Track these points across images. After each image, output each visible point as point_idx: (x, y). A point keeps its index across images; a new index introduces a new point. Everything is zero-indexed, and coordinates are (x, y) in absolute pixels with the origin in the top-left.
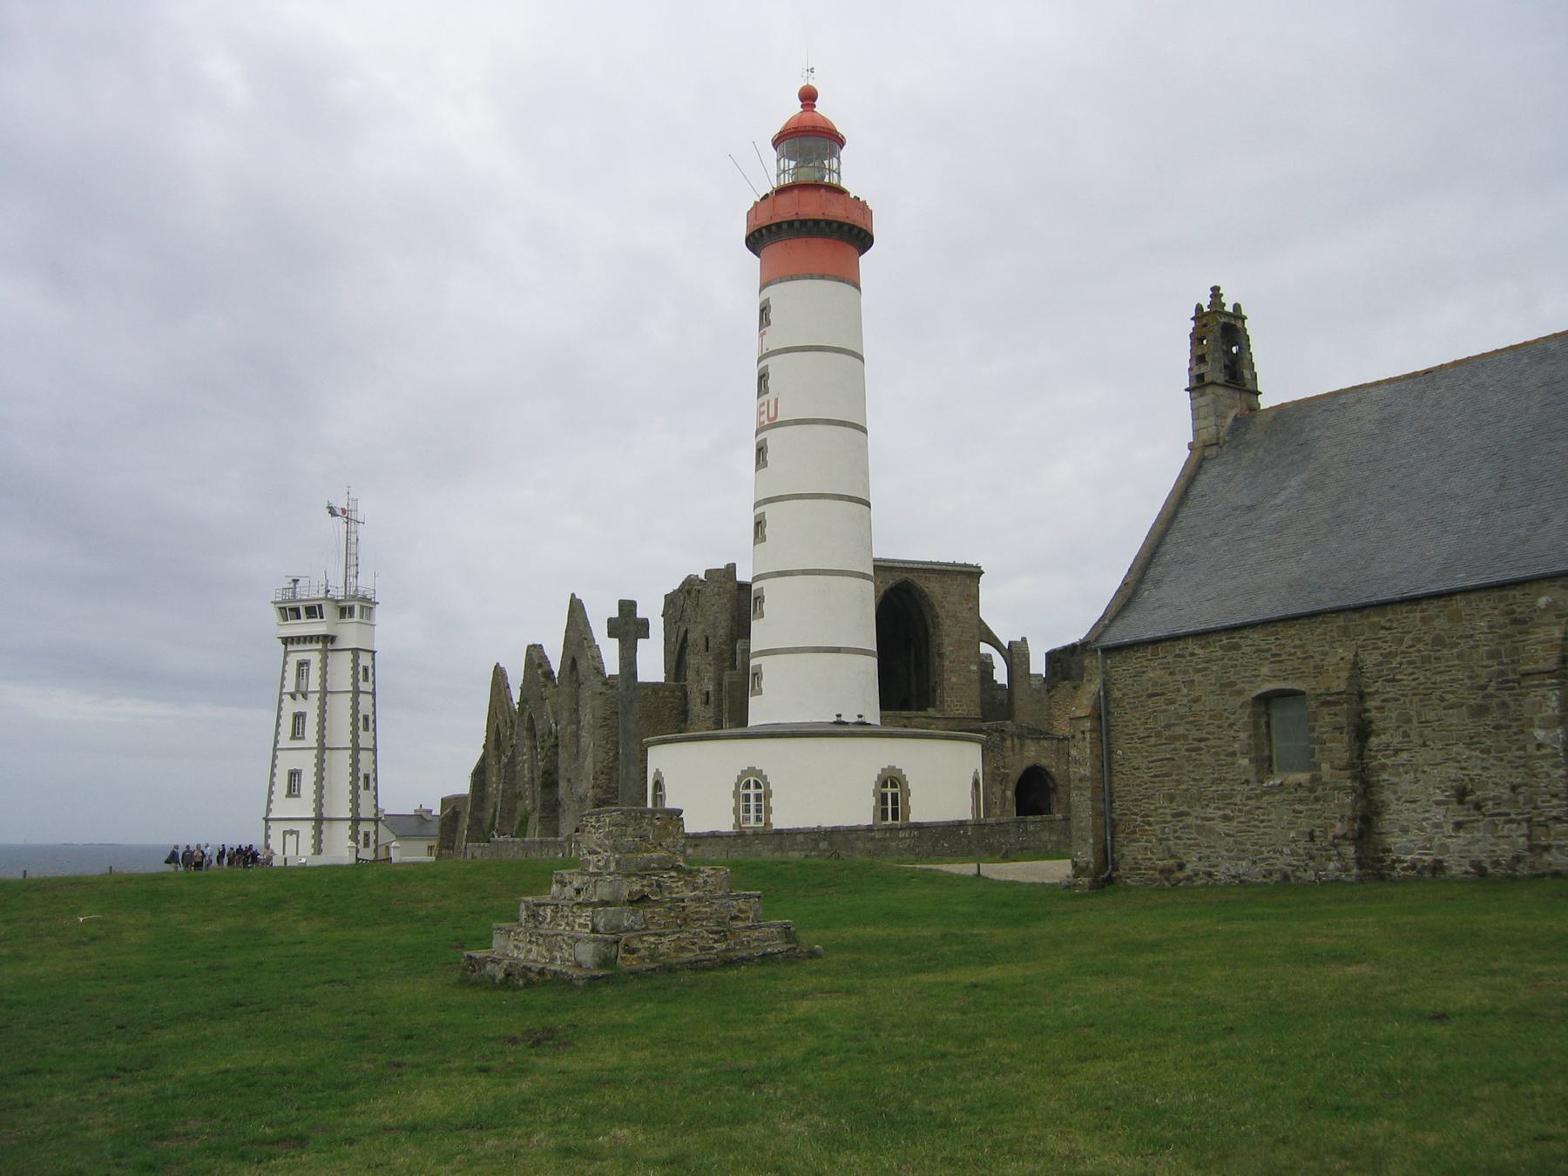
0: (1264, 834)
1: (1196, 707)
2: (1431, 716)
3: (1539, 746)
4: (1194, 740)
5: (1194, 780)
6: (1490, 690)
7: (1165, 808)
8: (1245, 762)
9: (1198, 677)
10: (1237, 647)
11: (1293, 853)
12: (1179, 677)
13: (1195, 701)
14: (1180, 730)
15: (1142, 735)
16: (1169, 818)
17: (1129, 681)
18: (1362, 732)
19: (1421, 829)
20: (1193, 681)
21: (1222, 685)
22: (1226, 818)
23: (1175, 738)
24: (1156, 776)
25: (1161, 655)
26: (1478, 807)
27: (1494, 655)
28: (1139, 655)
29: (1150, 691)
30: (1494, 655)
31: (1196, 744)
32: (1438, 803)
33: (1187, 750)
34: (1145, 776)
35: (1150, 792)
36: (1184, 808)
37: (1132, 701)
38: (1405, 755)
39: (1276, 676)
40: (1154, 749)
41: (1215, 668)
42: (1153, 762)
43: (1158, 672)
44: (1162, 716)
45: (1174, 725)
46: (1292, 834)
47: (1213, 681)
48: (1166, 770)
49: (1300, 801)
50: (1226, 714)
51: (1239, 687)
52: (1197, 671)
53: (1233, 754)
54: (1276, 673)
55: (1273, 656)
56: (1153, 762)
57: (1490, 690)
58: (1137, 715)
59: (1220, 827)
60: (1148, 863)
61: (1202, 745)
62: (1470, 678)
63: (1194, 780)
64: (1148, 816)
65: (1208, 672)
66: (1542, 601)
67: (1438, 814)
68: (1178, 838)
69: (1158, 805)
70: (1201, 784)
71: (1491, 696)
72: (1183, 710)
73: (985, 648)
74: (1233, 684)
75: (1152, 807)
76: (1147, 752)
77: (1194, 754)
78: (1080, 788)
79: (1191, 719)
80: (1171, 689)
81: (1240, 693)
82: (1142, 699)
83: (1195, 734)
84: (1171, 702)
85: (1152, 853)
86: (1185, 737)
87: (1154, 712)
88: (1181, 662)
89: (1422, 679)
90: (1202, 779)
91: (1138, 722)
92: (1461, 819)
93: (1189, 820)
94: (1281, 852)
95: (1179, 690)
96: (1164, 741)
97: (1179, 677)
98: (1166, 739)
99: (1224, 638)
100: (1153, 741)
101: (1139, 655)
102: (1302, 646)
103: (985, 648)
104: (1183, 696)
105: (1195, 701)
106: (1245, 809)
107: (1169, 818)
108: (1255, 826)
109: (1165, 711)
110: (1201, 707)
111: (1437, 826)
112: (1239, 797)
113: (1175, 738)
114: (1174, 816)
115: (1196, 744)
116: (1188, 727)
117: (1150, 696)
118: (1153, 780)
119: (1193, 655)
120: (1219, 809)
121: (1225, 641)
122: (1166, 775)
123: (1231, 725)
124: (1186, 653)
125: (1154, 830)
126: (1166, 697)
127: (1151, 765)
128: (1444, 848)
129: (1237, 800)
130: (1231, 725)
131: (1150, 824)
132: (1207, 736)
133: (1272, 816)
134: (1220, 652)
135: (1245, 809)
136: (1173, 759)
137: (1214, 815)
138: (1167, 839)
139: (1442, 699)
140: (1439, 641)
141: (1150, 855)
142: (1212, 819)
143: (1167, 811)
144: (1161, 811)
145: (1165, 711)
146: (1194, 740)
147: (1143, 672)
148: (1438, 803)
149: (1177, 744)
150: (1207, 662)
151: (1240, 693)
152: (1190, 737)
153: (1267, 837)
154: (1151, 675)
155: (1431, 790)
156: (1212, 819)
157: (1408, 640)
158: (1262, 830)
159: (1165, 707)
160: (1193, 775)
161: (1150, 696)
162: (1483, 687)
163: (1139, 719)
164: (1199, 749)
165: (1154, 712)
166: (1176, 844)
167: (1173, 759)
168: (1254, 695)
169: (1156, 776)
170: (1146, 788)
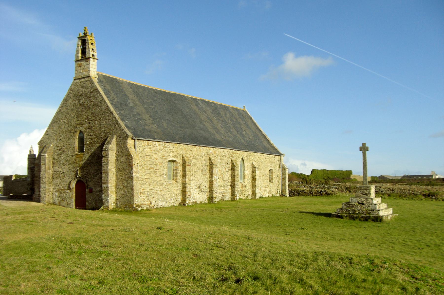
0: (168, 195)
1: (157, 161)
2: (196, 170)
4: (156, 169)
5: (155, 180)
6: (204, 167)
7: (148, 187)
8: (165, 176)
9: (157, 153)
10: (166, 147)
11: (174, 199)
12: (153, 152)
13: (157, 159)
14: (152, 166)
15: (144, 166)
16: (149, 190)
17: (141, 150)
20: (156, 154)
21: (162, 156)
22: (161, 190)
23: (151, 168)
24: (146, 178)
25: (149, 145)
26: (201, 190)
29: (146, 154)
31: (156, 171)
32: (196, 189)
33: (154, 172)
35: (145, 183)
36: (152, 188)
37: (141, 156)
41: (161, 151)
42: (146, 174)
43: (149, 150)
44: (148, 162)
46: (173, 195)
48: (149, 177)
50: (162, 164)
51: (166, 157)
52: (157, 151)
53: (163, 174)
55: (173, 151)
56: (146, 174)
57: (204, 167)
58: (143, 160)
59: (160, 193)
60: (144, 203)
61: (157, 171)
62: (202, 164)
64: (144, 189)
65: (160, 152)
66: (211, 151)
68: (151, 196)
70: (156, 181)
74: (164, 156)
75: (145, 187)
76: (144, 171)
77: (155, 173)
78: (137, 180)
79: (155, 164)
80: (151, 155)
81: (166, 159)
82: (144, 156)
83: (155, 168)
84: (151, 158)
85: (145, 200)
86: (154, 168)
87: (147, 160)
88: (154, 148)
89: (195, 163)
90: (156, 180)
91: (143, 162)
92: (199, 192)
93: (153, 191)
94: (171, 200)
95: (153, 155)
97: (153, 152)
98: (149, 168)
99: (164, 144)
100: (146, 168)
101: (144, 143)
102: (178, 150)
104: (153, 157)
105: (157, 159)
106: (165, 188)
107: (149, 190)
109: (150, 160)
110: (157, 161)
111: (196, 194)
112: (164, 185)
113: (151, 168)
115: (156, 171)
116: (154, 166)
117: (146, 155)
119: (157, 147)
120: (160, 188)
121: (164, 145)
123: (163, 167)
124: (155, 146)
125: (145, 193)
126: (150, 156)
129: (164, 186)
130: (163, 167)
131: (144, 192)
132: (158, 169)
134: (163, 148)
135: (165, 188)
136: (150, 174)
137: (158, 190)
138: (148, 196)
139: (198, 167)
141: (144, 201)
142: (158, 191)
143: (148, 188)
144: (147, 188)
145: (150, 160)
146: (156, 169)
147: (145, 148)
148: (196, 189)
149: (152, 170)
150: (159, 149)
151: (166, 159)
152: (155, 169)
154: (147, 150)
156: (158, 191)
158: (168, 194)
159: (149, 159)
160: (154, 179)
161: (146, 155)
162: (203, 166)
163: (143, 161)
164: (156, 172)
165: (147, 160)
166: (150, 197)
167: (150, 174)
168: (168, 160)
169: (146, 178)
170: (144, 182)
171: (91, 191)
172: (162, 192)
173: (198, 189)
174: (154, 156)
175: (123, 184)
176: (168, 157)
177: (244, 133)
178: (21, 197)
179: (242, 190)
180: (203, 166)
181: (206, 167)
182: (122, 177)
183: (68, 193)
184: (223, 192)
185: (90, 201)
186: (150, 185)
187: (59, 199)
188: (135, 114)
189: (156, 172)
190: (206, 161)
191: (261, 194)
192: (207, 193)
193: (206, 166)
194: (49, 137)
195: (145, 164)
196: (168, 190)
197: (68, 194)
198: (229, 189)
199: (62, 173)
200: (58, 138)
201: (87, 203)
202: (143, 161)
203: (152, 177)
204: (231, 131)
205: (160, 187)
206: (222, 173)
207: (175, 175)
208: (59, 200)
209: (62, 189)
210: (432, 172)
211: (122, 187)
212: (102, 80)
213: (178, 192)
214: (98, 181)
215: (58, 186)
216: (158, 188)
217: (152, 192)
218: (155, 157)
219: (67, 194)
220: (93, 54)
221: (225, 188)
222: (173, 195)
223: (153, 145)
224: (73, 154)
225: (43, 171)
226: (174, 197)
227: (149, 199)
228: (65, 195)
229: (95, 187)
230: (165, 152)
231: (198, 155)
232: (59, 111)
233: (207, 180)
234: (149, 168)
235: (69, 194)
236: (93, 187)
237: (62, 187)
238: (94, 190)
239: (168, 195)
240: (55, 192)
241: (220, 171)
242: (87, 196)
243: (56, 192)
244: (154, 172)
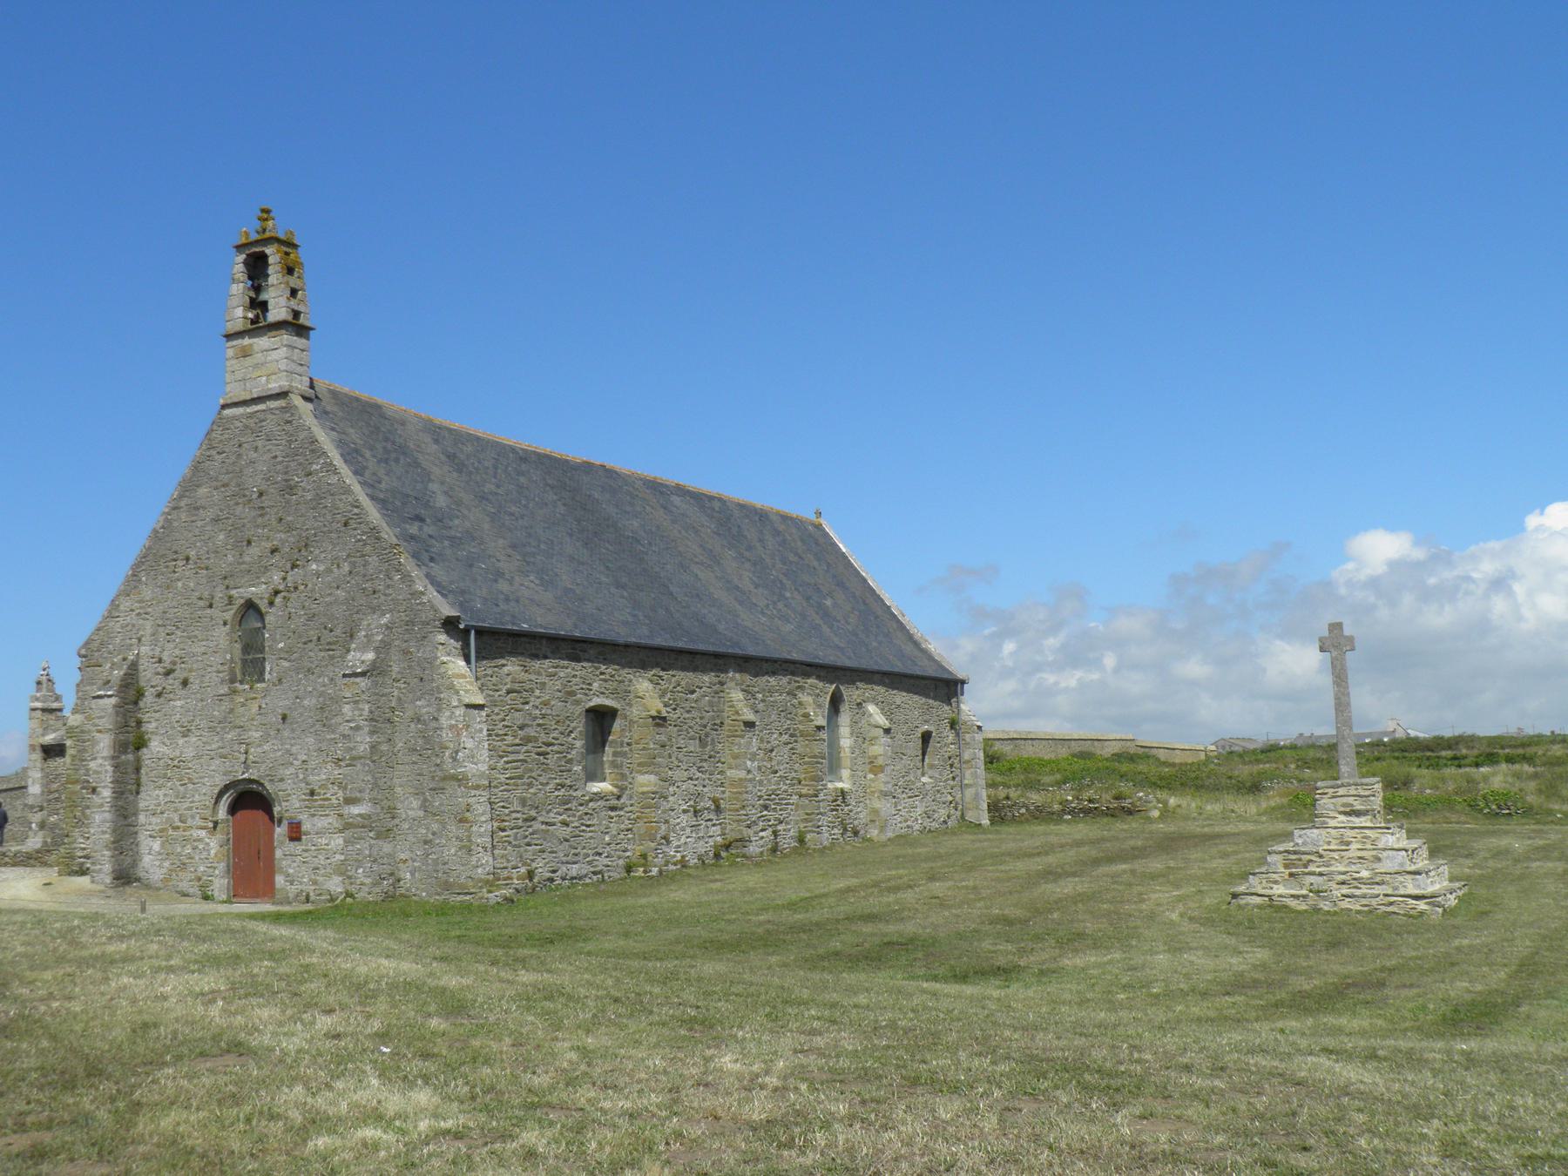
0: (591, 838)
2: (682, 743)
4: (543, 743)
5: (542, 784)
7: (518, 812)
13: (545, 704)
14: (531, 732)
16: (520, 823)
22: (566, 824)
28: (499, 644)
31: (544, 749)
32: (685, 811)
33: (538, 754)
34: (501, 776)
39: (603, 693)
40: (510, 749)
45: (527, 725)
47: (559, 687)
54: (603, 690)
63: (542, 784)
69: (512, 809)
77: (542, 758)
81: (578, 702)
83: (543, 737)
85: (508, 861)
93: (537, 826)
96: (517, 741)
106: (578, 814)
107: (520, 823)
108: (583, 831)
114: (526, 820)
118: (508, 781)
122: (520, 777)
127: (507, 766)
133: (595, 821)
136: (526, 761)
143: (519, 815)
144: (514, 815)
146: (543, 743)
151: (578, 702)
153: (592, 841)
155: (680, 802)
168: (587, 707)
171: (295, 834)
172: (569, 829)
174: (537, 692)
175: (425, 800)
176: (586, 694)
177: (828, 602)
178: (7, 859)
179: (837, 810)
180: (705, 726)
181: (716, 730)
182: (420, 775)
183: (200, 840)
184: (776, 819)
185: (291, 871)
187: (166, 864)
188: (458, 535)
189: (548, 753)
190: (715, 709)
191: (899, 820)
192: (720, 824)
193: (715, 724)
194: (122, 628)
195: (506, 723)
196: (589, 819)
197: (201, 847)
198: (793, 807)
199: (176, 763)
200: (161, 629)
201: (279, 880)
202: (498, 714)
204: (787, 599)
206: (772, 751)
207: (613, 762)
208: (165, 871)
209: (179, 824)
210: (1519, 729)
211: (421, 813)
212: (328, 408)
213: (623, 826)
214: (323, 792)
215: (162, 813)
216: (552, 815)
217: (530, 830)
218: (539, 698)
219: (196, 844)
220: (296, 308)
221: (781, 804)
222: (607, 838)
223: (534, 651)
224: (222, 692)
225: (103, 758)
226: (609, 844)
227: (521, 857)
228: (188, 850)
229: (313, 815)
230: (575, 676)
232: (163, 527)
233: (719, 776)
234: (521, 739)
235: (208, 844)
236: (303, 817)
237: (176, 819)
238: (306, 827)
239: (591, 838)
240: (151, 836)
241: (762, 741)
242: (278, 853)
243: (155, 837)
244: (538, 754)
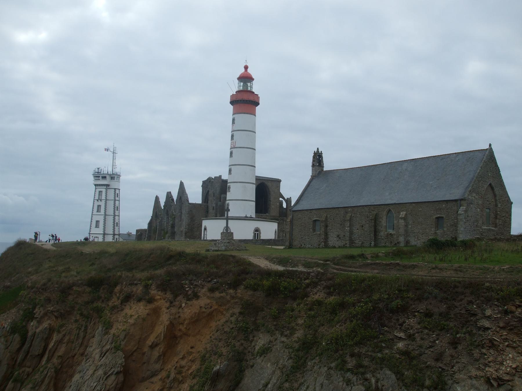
1: (305, 221)
2: (335, 225)
3: (346, 230)
8: (311, 230)
9: (306, 217)
10: (311, 212)
11: (317, 244)
18: (327, 226)
19: (333, 241)
22: (308, 238)
23: (302, 226)
26: (340, 238)
27: (343, 217)
30: (343, 217)
31: (305, 227)
36: (303, 237)
38: (332, 230)
46: (317, 241)
49: (318, 236)
53: (310, 229)
59: (307, 240)
67: (335, 239)
71: (342, 223)
72: (303, 221)
73: (281, 199)
84: (302, 220)
93: (303, 238)
95: (303, 218)
103: (281, 199)
111: (335, 241)
113: (302, 226)
128: (336, 244)
140: (337, 214)
148: (335, 237)
157: (333, 214)
162: (342, 221)
173: (337, 238)
180: (342, 221)
186: (301, 235)
203: (302, 230)
205: (308, 236)
231: (337, 214)
